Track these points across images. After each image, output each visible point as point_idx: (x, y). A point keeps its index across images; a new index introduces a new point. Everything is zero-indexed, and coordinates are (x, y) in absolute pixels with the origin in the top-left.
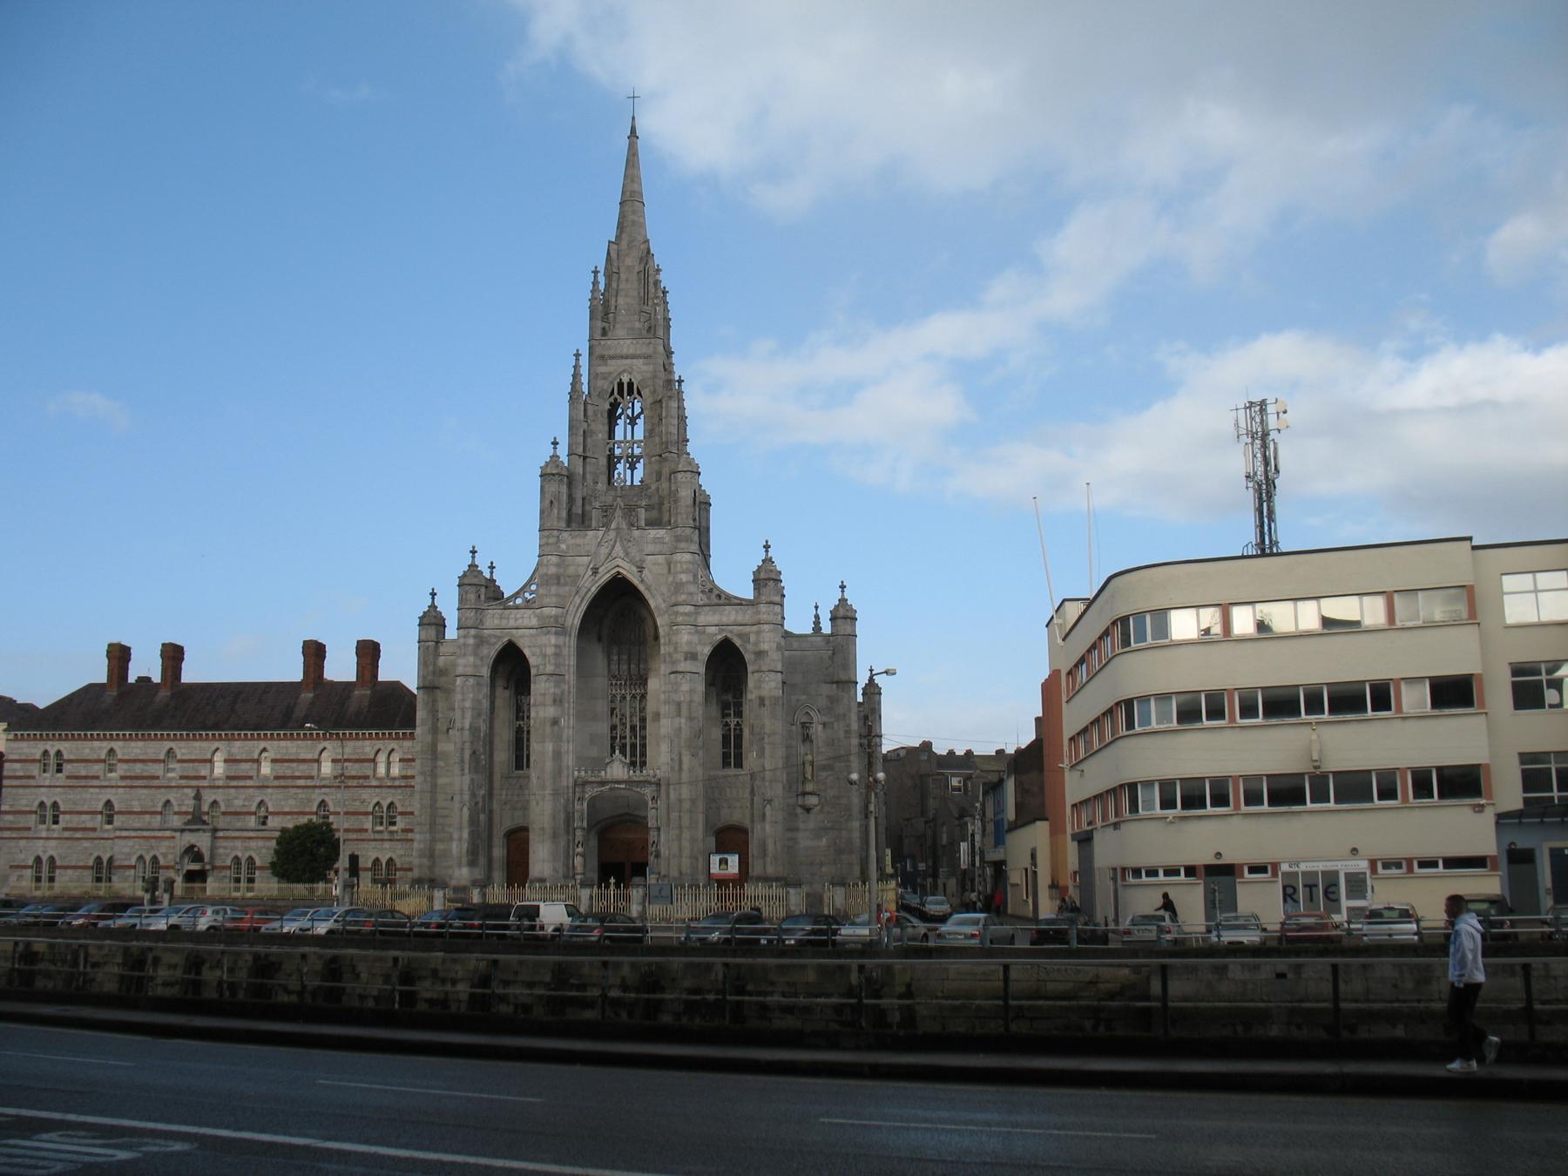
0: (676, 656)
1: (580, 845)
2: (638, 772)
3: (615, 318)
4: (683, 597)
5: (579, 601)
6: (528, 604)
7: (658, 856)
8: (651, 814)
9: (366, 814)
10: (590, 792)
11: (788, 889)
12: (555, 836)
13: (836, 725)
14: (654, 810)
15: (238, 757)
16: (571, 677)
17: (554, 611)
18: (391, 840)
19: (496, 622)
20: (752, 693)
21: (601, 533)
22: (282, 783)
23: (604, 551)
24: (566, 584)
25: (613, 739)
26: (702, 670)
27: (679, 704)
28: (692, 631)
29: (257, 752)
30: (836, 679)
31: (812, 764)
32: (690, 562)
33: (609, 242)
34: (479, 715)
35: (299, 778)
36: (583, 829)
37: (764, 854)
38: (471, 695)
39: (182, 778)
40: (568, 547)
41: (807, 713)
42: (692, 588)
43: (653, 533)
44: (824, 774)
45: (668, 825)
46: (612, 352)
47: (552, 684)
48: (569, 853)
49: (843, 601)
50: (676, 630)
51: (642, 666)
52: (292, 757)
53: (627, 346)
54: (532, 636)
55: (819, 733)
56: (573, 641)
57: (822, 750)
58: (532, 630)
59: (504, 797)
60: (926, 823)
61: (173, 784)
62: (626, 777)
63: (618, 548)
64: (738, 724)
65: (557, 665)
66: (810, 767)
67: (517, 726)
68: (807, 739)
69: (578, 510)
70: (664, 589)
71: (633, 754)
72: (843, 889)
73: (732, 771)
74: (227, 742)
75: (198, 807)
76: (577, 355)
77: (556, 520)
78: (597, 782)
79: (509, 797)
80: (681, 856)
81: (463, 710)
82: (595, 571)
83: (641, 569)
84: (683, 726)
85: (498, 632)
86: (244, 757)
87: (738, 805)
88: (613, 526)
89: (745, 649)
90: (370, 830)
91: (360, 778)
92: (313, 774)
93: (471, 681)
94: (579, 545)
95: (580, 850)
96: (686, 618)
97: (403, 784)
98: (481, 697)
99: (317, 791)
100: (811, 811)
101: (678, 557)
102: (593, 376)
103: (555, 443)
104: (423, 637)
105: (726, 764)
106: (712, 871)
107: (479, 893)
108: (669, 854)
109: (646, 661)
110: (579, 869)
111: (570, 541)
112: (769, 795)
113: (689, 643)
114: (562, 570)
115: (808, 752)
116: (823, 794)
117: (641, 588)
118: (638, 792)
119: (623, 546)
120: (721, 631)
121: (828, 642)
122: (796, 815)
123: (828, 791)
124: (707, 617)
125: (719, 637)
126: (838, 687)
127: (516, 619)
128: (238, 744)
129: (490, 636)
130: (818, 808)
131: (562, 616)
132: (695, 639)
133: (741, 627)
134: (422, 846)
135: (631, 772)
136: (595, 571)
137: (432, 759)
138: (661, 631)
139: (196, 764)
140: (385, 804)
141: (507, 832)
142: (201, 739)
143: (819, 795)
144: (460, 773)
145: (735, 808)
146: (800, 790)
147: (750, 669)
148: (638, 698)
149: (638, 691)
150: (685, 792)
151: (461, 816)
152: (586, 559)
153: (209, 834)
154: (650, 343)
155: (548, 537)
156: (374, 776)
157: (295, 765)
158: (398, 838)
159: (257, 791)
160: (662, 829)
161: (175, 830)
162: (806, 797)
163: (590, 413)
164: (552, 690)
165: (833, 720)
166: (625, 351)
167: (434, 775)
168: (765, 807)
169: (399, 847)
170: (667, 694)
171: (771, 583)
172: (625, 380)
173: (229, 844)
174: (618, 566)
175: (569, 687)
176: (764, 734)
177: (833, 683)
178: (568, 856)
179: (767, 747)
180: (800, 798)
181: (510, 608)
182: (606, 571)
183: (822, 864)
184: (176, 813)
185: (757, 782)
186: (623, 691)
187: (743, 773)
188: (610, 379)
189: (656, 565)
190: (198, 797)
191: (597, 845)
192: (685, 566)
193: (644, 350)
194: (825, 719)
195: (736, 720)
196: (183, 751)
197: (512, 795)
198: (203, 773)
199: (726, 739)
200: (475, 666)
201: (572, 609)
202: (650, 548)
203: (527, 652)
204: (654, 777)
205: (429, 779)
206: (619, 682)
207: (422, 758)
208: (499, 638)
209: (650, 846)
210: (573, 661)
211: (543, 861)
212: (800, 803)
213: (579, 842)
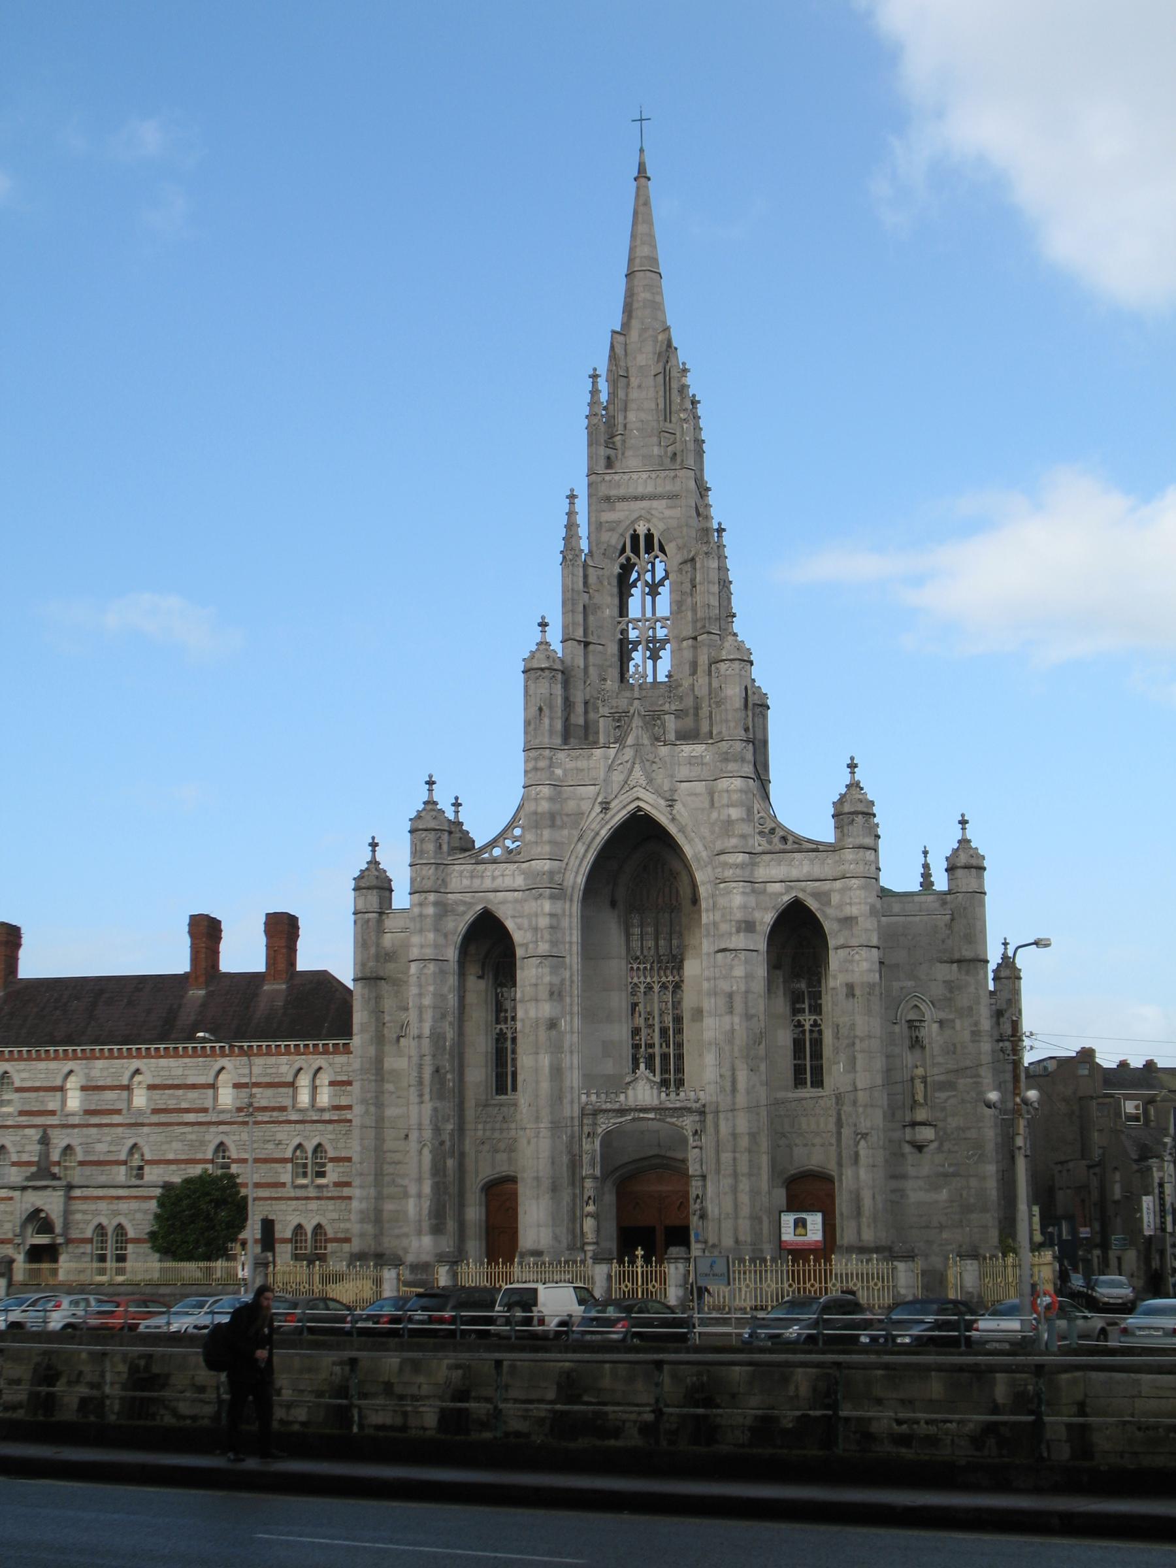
0: (724, 927)
1: (591, 1202)
2: (673, 1095)
3: (624, 441)
4: (734, 841)
5: (582, 851)
6: (511, 856)
7: (703, 1216)
8: (693, 1155)
9: (284, 1161)
10: (605, 1124)
11: (895, 1263)
12: (554, 1189)
14: (697, 1150)
15: (100, 1083)
16: (574, 960)
17: (547, 865)
18: (318, 1198)
19: (466, 882)
20: (835, 977)
21: (612, 752)
22: (163, 1118)
23: (617, 777)
24: (562, 827)
25: (636, 1047)
26: (762, 946)
27: (730, 996)
28: (748, 890)
29: (128, 1074)
30: (957, 956)
31: (924, 1080)
32: (741, 791)
33: (614, 332)
34: (443, 1016)
35: (187, 1111)
36: (595, 1178)
37: (858, 1213)
38: (431, 988)
39: (22, 1113)
40: (565, 775)
41: (916, 1006)
42: (746, 829)
43: (688, 750)
44: (942, 1095)
45: (718, 1171)
46: (622, 492)
47: (547, 970)
48: (574, 1213)
49: (964, 842)
50: (725, 888)
51: (675, 942)
52: (176, 1082)
53: (642, 483)
54: (516, 901)
55: (934, 1035)
56: (576, 908)
57: (940, 1060)
58: (517, 893)
59: (480, 1133)
61: (9, 1123)
62: (656, 1102)
63: (638, 773)
64: (815, 1024)
65: (554, 943)
66: (922, 1085)
67: (498, 1031)
68: (916, 1043)
69: (578, 719)
70: (705, 831)
71: (665, 1070)
73: (808, 1092)
74: (84, 1062)
75: (45, 1155)
76: (572, 497)
77: (547, 734)
78: (614, 1110)
79: (488, 1133)
80: (736, 1218)
81: (421, 1009)
82: (605, 807)
83: (671, 803)
84: (737, 1027)
85: (467, 897)
86: (109, 1082)
87: (817, 1141)
88: (630, 740)
89: (824, 912)
90: (289, 1185)
91: (274, 1109)
92: (206, 1106)
93: (431, 967)
94: (582, 770)
95: (591, 1208)
96: (738, 871)
97: (336, 1118)
98: (445, 990)
99: (213, 1129)
100: (925, 1150)
101: (723, 784)
102: (597, 527)
103: (543, 625)
104: (360, 907)
105: (799, 1082)
106: (785, 1238)
107: (448, 1272)
108: (720, 1214)
109: (681, 935)
110: (590, 1236)
111: (570, 765)
112: (864, 1126)
113: (744, 907)
114: (558, 806)
115: (918, 1064)
116: (940, 1124)
117: (672, 829)
118: (673, 1124)
119: (643, 769)
121: (944, 903)
122: (903, 1155)
123: (949, 1119)
124: (769, 870)
125: (786, 898)
127: (494, 878)
128: (100, 1064)
129: (456, 903)
131: (559, 872)
132: (752, 901)
134: (364, 1205)
135: (663, 1095)
136: (605, 807)
137: (376, 1081)
138: (703, 891)
139: (42, 1094)
140: (309, 1147)
141: (487, 1183)
142: (48, 1059)
143: (935, 1125)
144: (416, 1100)
145: (813, 1145)
146: (908, 1119)
147: (832, 943)
148: (671, 987)
149: (670, 978)
150: (743, 1124)
151: (420, 1161)
152: (592, 790)
153: (61, 1193)
154: (676, 476)
155: (536, 759)
156: (294, 1107)
157: (180, 1092)
158: (330, 1195)
159: (127, 1131)
160: (709, 1177)
161: (13, 1188)
163: (592, 580)
164: (547, 979)
165: (951, 1016)
166: (640, 490)
167: (379, 1105)
168: (858, 1142)
169: (331, 1208)
170: (712, 982)
171: (860, 819)
172: (642, 530)
173: (91, 1206)
174: (638, 799)
175: (571, 976)
176: (855, 1037)
177: (952, 962)
178: (575, 1218)
179: (859, 1056)
180: (908, 1130)
181: (483, 862)
182: (621, 806)
183: (941, 1227)
184: (14, 1164)
185: (845, 1108)
187: (824, 1094)
188: (620, 531)
189: (691, 796)
190: (45, 1141)
191: (615, 1202)
192: (735, 797)
193: (669, 487)
194: (942, 1015)
195: (813, 1017)
196: (24, 1075)
197: (493, 1130)
198: (51, 1106)
199: (798, 1045)
200: (436, 946)
201: (574, 863)
202: (684, 772)
203: (510, 925)
204: (697, 1101)
205: (372, 1109)
206: (642, 966)
207: (362, 1080)
208: (470, 905)
209: (692, 1202)
210: (575, 937)
211: (539, 1226)
212: (908, 1138)
213: (589, 1198)
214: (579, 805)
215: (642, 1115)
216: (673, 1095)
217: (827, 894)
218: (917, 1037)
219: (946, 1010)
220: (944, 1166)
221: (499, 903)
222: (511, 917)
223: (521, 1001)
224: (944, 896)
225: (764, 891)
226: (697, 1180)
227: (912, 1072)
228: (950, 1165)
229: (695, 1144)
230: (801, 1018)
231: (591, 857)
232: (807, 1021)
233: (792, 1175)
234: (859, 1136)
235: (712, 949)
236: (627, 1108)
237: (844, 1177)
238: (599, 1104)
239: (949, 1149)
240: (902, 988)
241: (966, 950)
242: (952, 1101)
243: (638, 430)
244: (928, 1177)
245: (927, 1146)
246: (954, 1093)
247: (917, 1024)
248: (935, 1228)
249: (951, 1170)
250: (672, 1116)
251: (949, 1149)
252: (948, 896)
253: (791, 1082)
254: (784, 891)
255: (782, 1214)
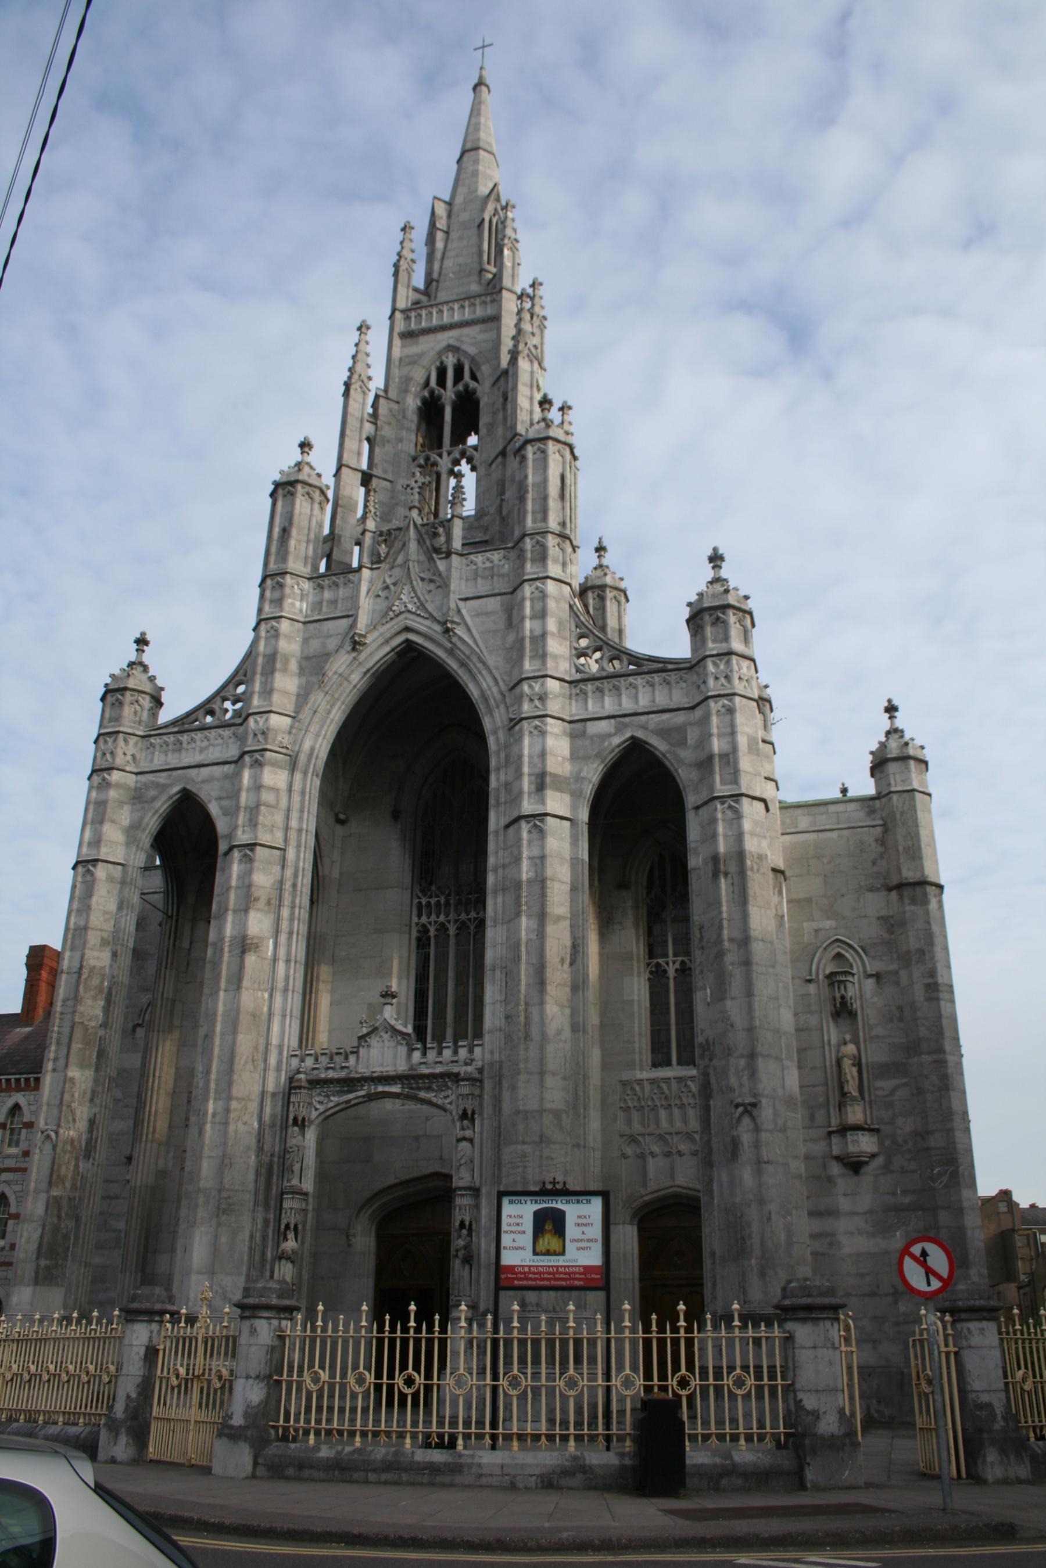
1: (291, 1235)
3: (437, 287)
7: (468, 1260)
11: (790, 1326)
13: (903, 975)
14: (465, 1144)
30: (895, 880)
31: (858, 1064)
41: (839, 955)
44: (888, 1084)
48: (263, 1254)
49: (894, 732)
57: (879, 1031)
60: (1019, 1288)
62: (402, 1067)
66: (854, 1070)
68: (843, 1011)
72: (990, 1327)
78: (338, 1081)
85: (162, 778)
105: (660, 1057)
106: (508, 1259)
115: (848, 1037)
116: (886, 1129)
117: (453, 664)
118: (429, 1102)
120: (618, 731)
121: (872, 811)
122: (830, 1179)
123: (900, 1121)
125: (617, 740)
126: (901, 897)
130: (880, 1161)
133: (665, 716)
135: (417, 1055)
143: (877, 1131)
145: (680, 1154)
146: (835, 1122)
148: (472, 927)
149: (473, 915)
162: (850, 1136)
165: (893, 967)
168: (739, 1120)
177: (890, 889)
180: (835, 1139)
186: (442, 918)
195: (680, 959)
206: (433, 901)
208: (163, 787)
209: (454, 1234)
212: (836, 1151)
213: (287, 1227)
214: (324, 645)
215: (380, 1089)
216: (432, 1055)
217: (681, 730)
218: (843, 997)
219: (884, 958)
220: (894, 1194)
221: (203, 782)
222: (216, 799)
223: (215, 918)
224: (871, 803)
225: (583, 733)
226: (462, 1195)
227: (838, 1051)
228: (905, 1192)
229: (460, 1134)
230: (660, 961)
231: (337, 716)
232: (671, 964)
233: (647, 1204)
234: (741, 1109)
235: (504, 821)
236: (357, 1076)
237: (715, 1187)
238: (316, 1072)
239: (902, 1167)
240: (817, 931)
241: (909, 869)
242: (901, 1093)
243: (453, 273)
244: (871, 1212)
245: (867, 1163)
246: (904, 1081)
247: (843, 978)
248: (887, 1295)
249: (907, 1200)
250: (429, 1089)
251: (902, 1167)
252: (877, 802)
253: (647, 1058)
254: (613, 731)
255: (505, 1201)
